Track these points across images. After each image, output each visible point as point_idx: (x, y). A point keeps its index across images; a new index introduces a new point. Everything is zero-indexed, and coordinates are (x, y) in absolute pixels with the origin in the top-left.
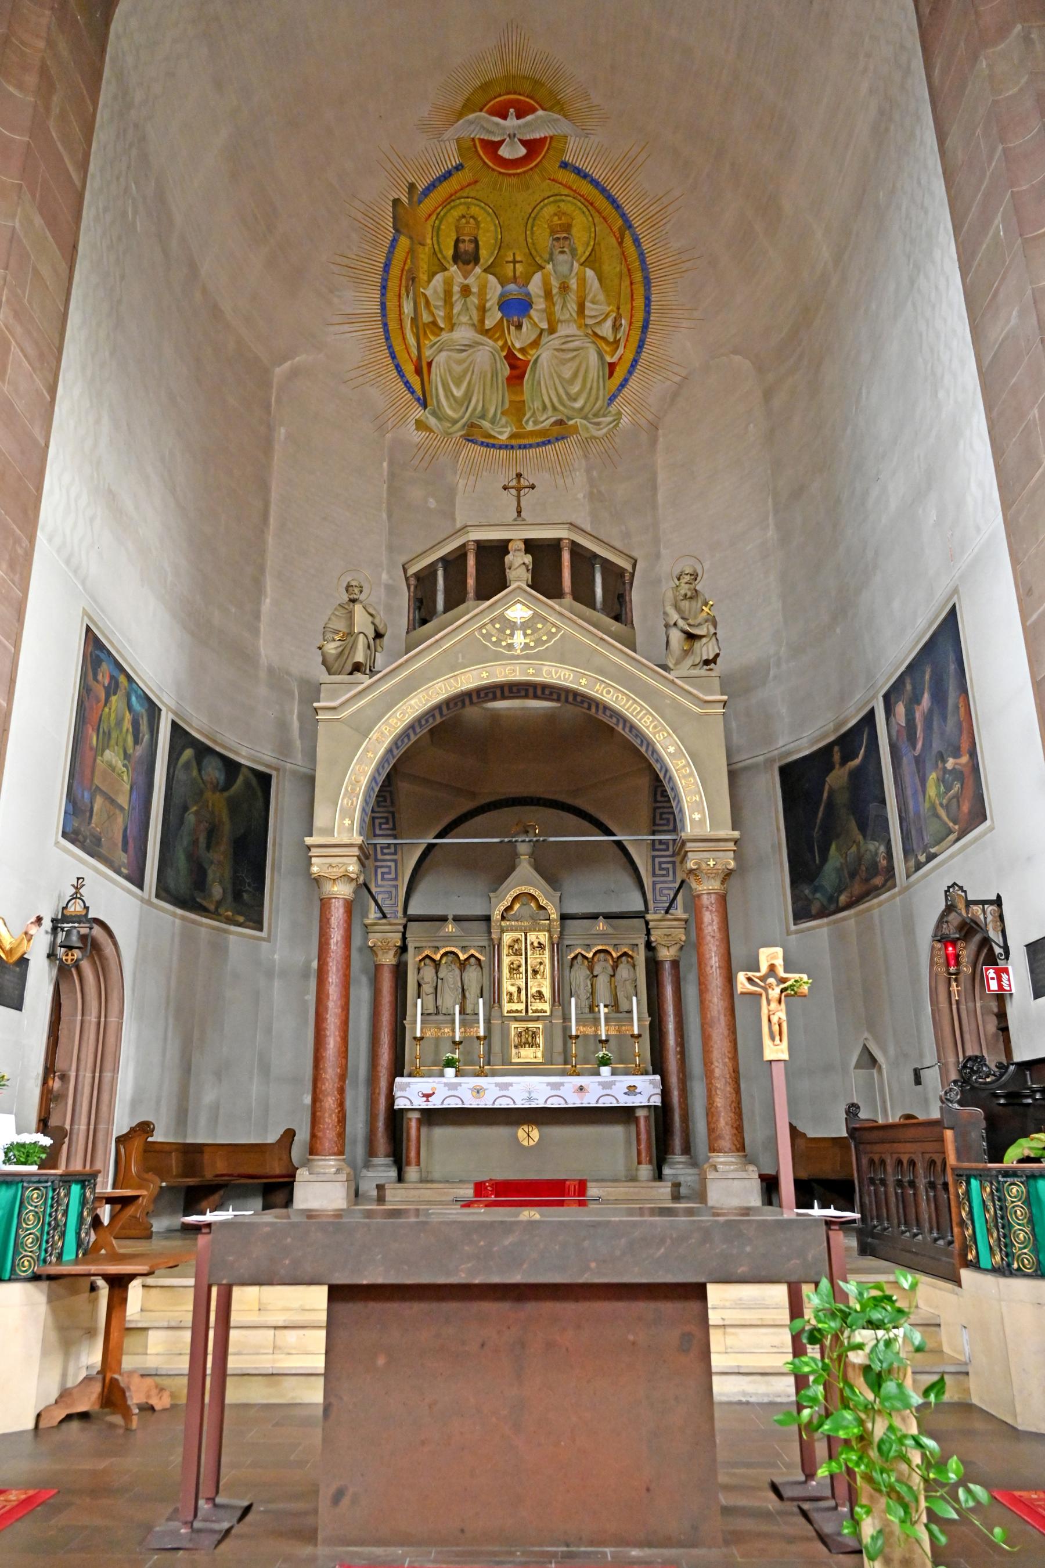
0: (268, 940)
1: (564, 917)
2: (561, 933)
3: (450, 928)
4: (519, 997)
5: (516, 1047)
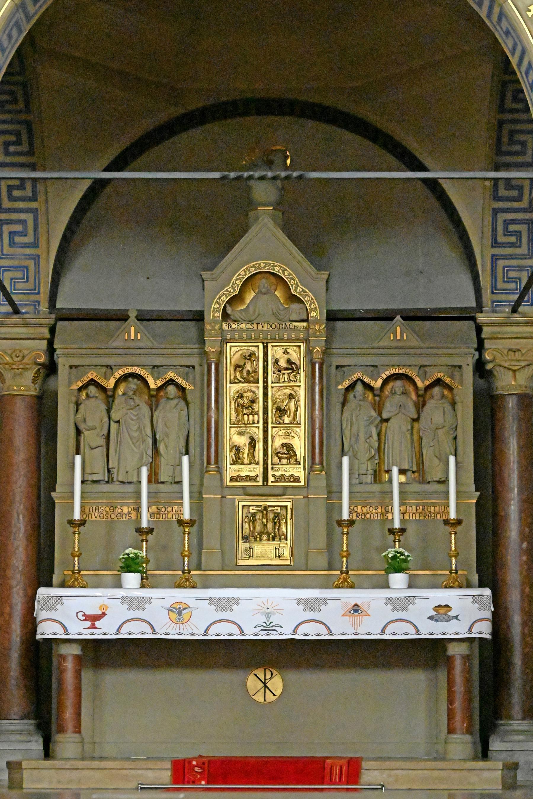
1: (332, 317)
2: (328, 342)
3: (132, 331)
4: (252, 454)
5: (246, 539)
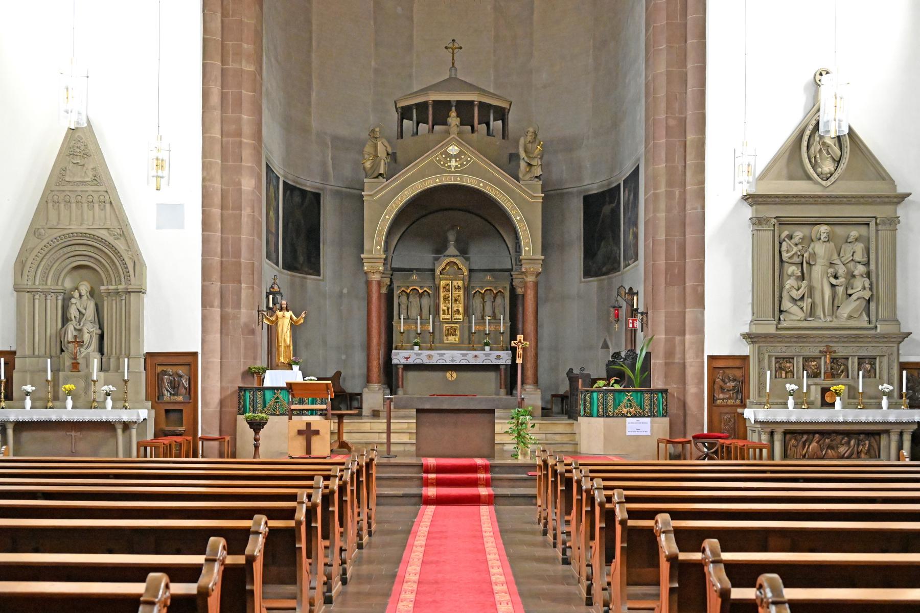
0: (323, 280)
1: (471, 271)
